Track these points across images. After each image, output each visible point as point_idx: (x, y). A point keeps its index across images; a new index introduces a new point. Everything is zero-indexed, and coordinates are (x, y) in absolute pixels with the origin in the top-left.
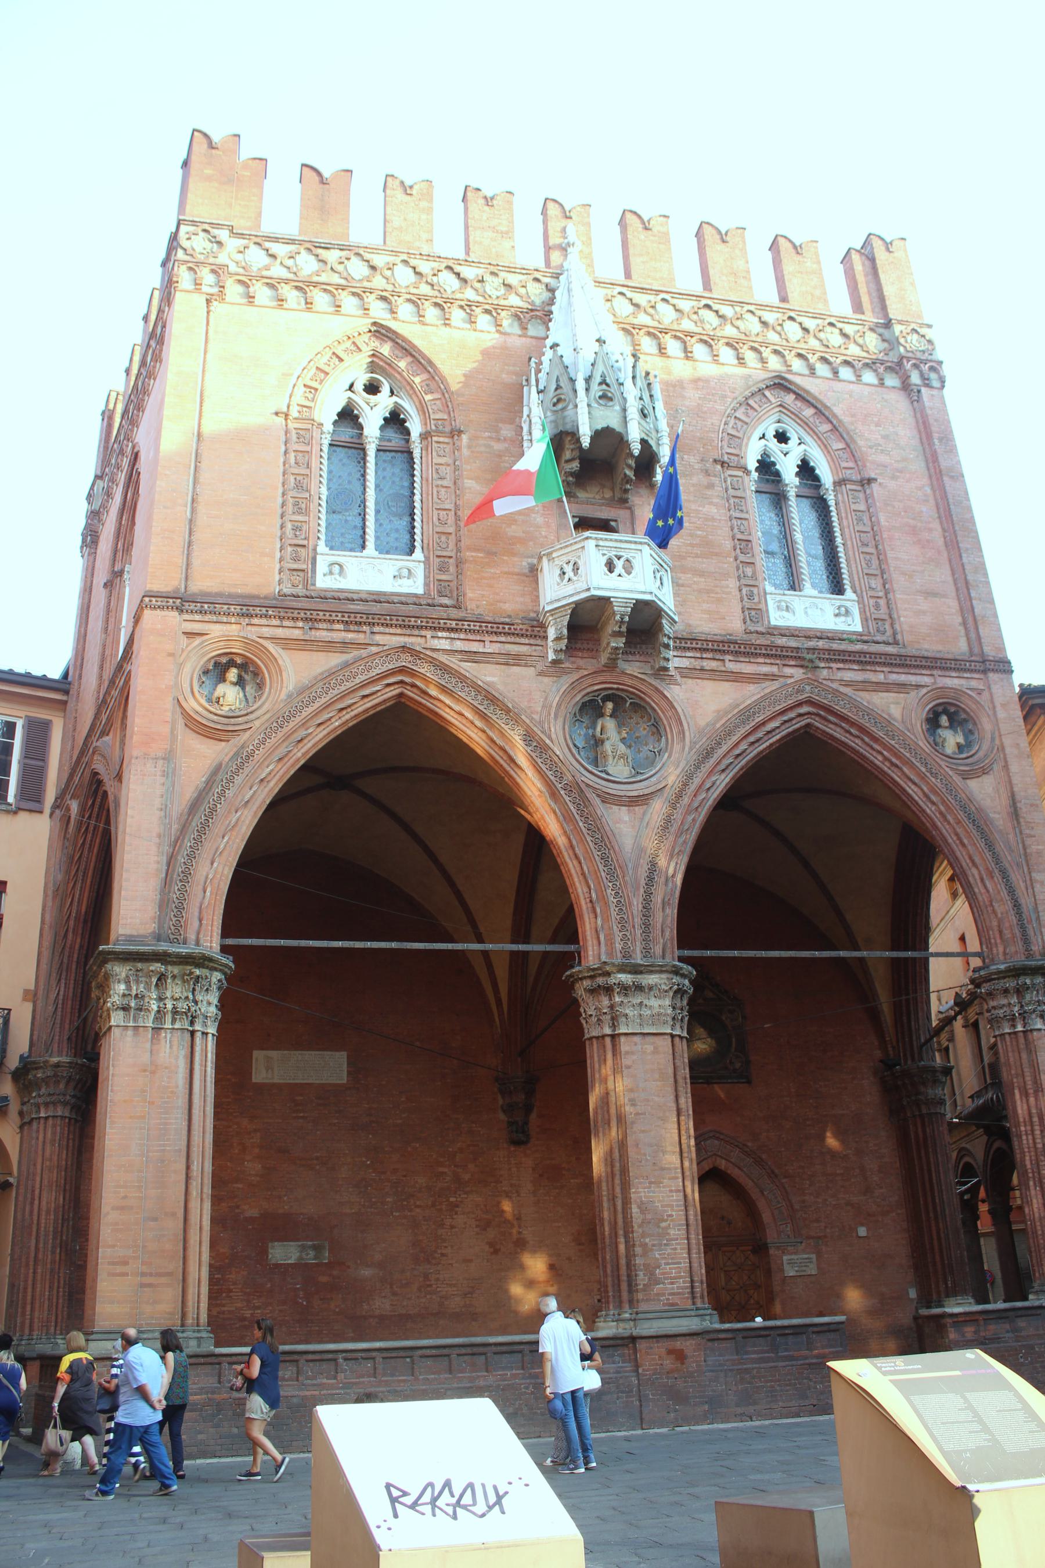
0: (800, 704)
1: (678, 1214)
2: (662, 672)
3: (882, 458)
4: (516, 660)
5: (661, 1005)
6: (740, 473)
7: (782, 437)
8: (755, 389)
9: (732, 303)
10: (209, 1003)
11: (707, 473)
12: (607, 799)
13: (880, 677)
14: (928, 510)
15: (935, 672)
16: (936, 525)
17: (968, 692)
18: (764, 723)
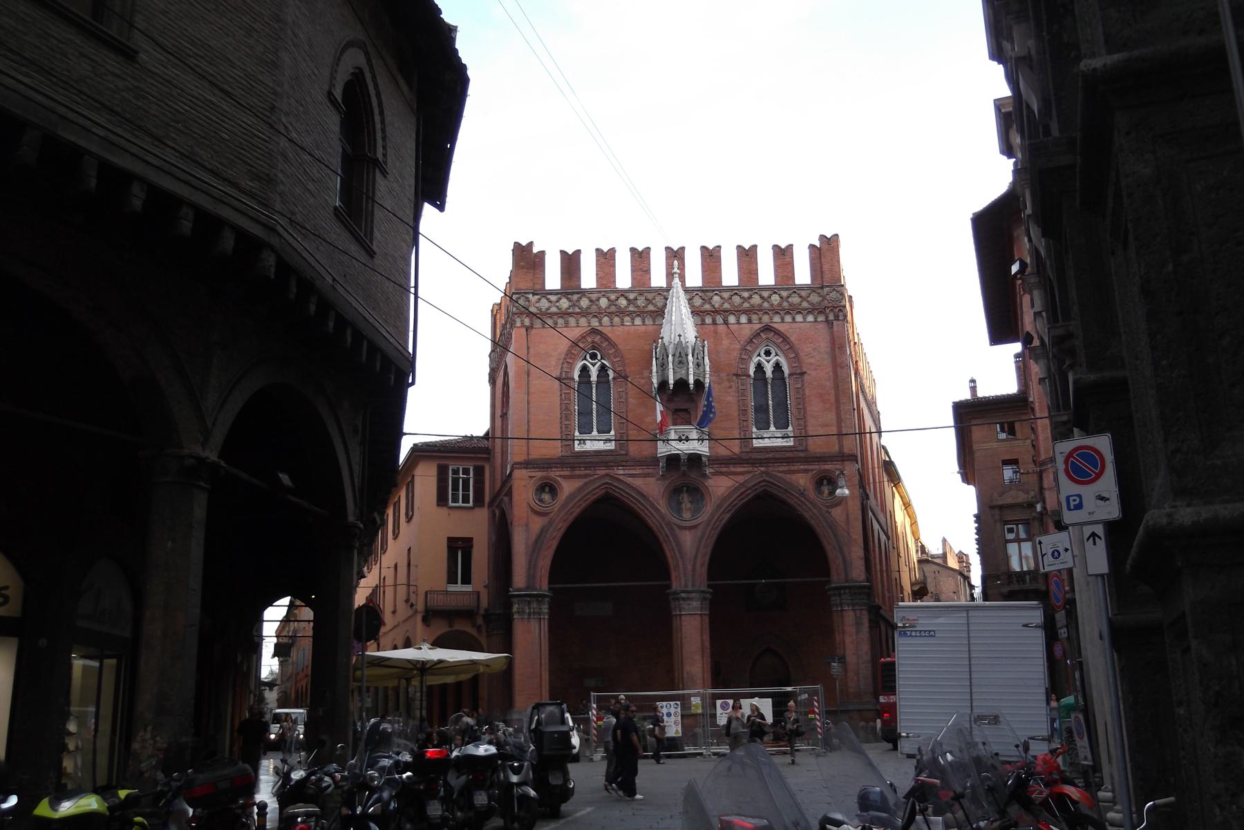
1: (700, 675)
2: (704, 476)
3: (812, 360)
5: (695, 604)
7: (768, 353)
9: (748, 290)
10: (545, 609)
11: (729, 381)
12: (681, 528)
14: (829, 384)
16: (833, 392)
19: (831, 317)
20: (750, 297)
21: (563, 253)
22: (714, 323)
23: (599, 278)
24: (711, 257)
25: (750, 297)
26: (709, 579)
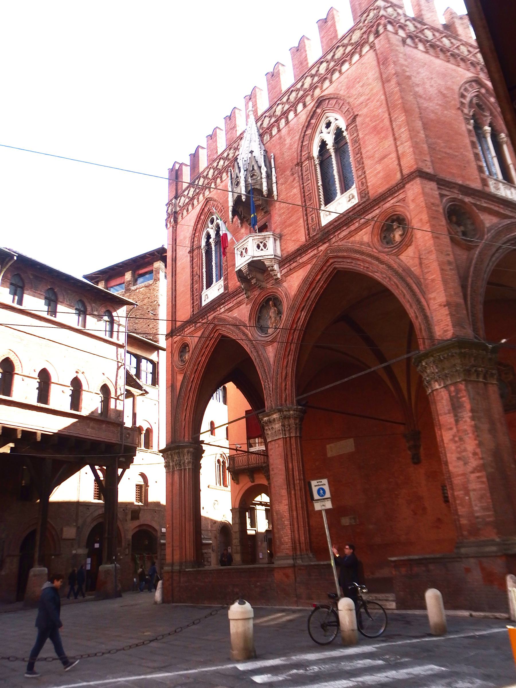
0: (327, 261)
2: (278, 282)
3: (362, 99)
4: (239, 304)
5: (277, 426)
8: (311, 114)
13: (357, 225)
15: (380, 205)
16: (386, 115)
17: (398, 204)
18: (314, 280)
19: (371, 38)
20: (302, 85)
22: (279, 131)
25: (302, 85)
26: (296, 397)
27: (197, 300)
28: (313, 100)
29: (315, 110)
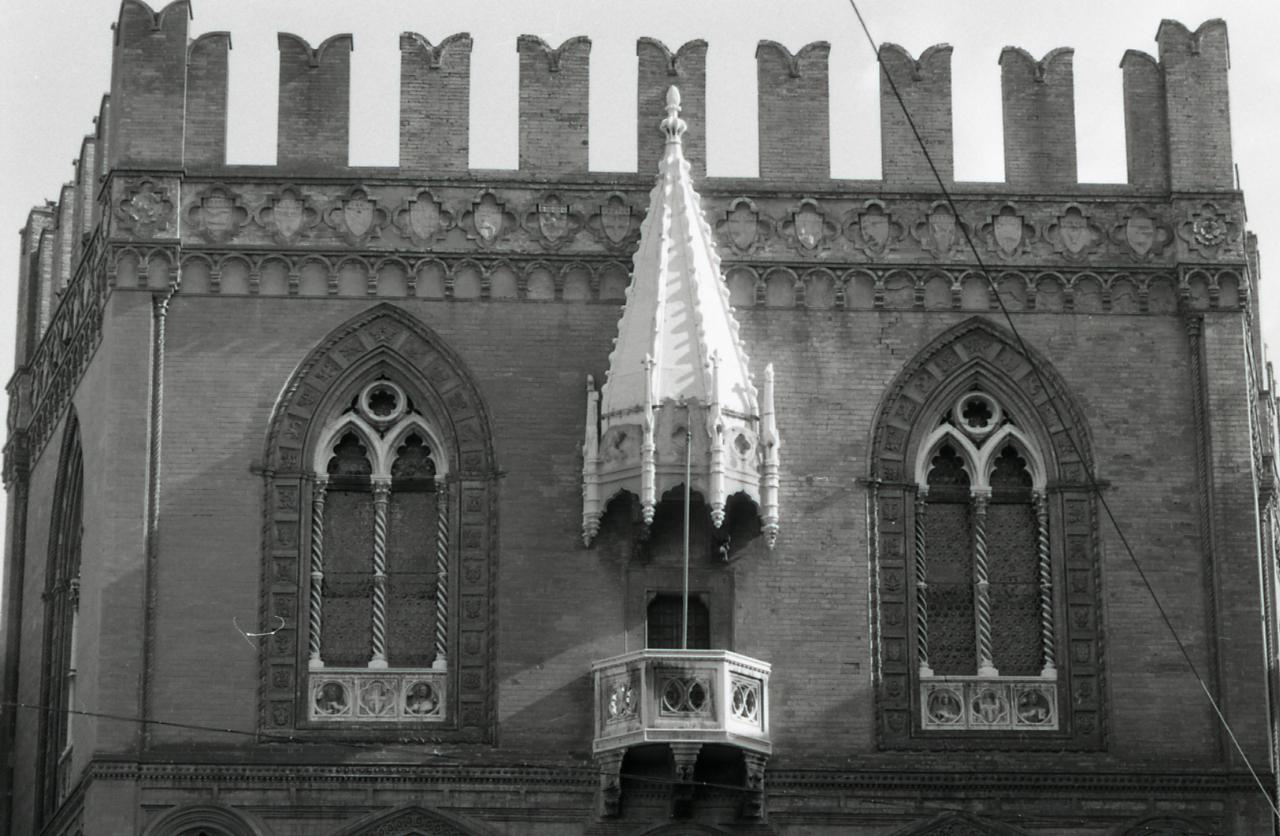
6: (898, 493)
21: (290, 45)
23: (408, 136)
24: (792, 79)
27: (281, 685)
28: (956, 309)
29: (950, 342)
